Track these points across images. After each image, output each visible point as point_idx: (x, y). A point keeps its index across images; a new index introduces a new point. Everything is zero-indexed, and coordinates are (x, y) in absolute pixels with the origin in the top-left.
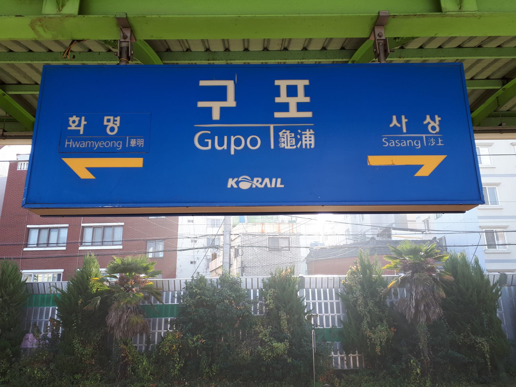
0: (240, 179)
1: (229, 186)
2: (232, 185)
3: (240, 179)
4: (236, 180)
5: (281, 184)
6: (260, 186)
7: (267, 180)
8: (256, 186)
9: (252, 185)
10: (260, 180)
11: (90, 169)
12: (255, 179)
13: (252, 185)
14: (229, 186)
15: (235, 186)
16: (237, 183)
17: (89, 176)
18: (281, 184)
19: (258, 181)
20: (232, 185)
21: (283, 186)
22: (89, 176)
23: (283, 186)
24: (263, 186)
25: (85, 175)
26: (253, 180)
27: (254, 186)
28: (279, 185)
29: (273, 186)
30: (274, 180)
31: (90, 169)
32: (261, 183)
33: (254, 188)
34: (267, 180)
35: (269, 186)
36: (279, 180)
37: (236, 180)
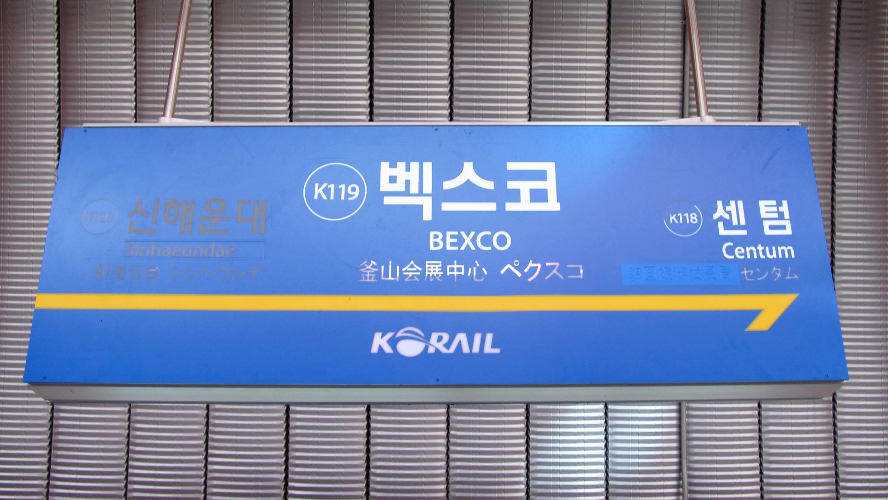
6: (444, 350)
7: (462, 337)
8: (437, 350)
9: (426, 348)
12: (435, 336)
13: (426, 348)
19: (440, 339)
24: (452, 349)
26: (427, 338)
27: (431, 350)
28: (488, 349)
32: (448, 346)
33: (431, 354)
34: (462, 337)
35: (466, 349)
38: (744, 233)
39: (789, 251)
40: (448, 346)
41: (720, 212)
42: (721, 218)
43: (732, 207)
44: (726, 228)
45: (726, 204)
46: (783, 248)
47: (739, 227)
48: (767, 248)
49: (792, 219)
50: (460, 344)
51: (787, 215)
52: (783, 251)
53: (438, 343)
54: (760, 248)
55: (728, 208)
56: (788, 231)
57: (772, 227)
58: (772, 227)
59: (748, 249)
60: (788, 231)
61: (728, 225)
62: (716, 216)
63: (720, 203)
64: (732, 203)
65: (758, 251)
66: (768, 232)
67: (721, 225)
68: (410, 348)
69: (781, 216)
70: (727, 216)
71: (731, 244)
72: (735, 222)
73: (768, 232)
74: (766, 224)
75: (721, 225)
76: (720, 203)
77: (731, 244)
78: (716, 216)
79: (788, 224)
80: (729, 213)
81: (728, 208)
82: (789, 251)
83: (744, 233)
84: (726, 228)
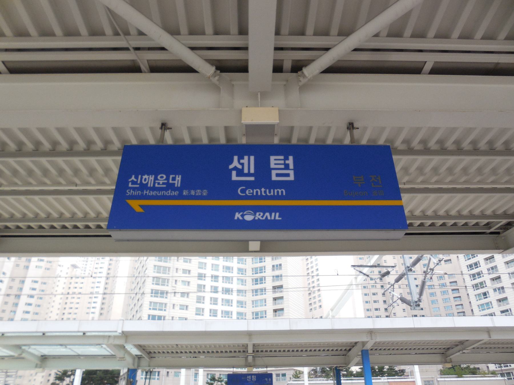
0: (245, 213)
1: (236, 218)
2: (238, 218)
6: (261, 219)
7: (267, 214)
9: (255, 218)
10: (262, 214)
12: (258, 214)
14: (236, 218)
15: (241, 218)
16: (242, 216)
18: (279, 217)
19: (260, 215)
20: (238, 218)
21: (280, 219)
23: (280, 219)
24: (264, 218)
26: (255, 214)
27: (256, 218)
28: (277, 218)
29: (273, 218)
30: (273, 214)
32: (262, 217)
35: (269, 218)
36: (277, 214)
37: (241, 213)
38: (252, 179)
39: (282, 192)
40: (262, 217)
41: (235, 163)
42: (235, 168)
43: (245, 161)
44: (237, 175)
45: (241, 158)
46: (279, 190)
47: (249, 175)
48: (268, 191)
49: (295, 169)
50: (267, 217)
51: (291, 166)
52: (278, 192)
53: (259, 216)
54: (263, 190)
55: (242, 161)
56: (292, 178)
57: (278, 175)
58: (278, 175)
59: (255, 191)
60: (292, 178)
61: (240, 173)
62: (231, 167)
63: (236, 158)
64: (246, 158)
65: (261, 192)
66: (274, 178)
67: (234, 173)
68: (249, 218)
69: (287, 167)
70: (240, 167)
71: (244, 187)
72: (246, 171)
73: (274, 178)
74: (274, 173)
75: (234, 173)
76: (236, 158)
77: (244, 187)
78: (231, 167)
79: (292, 173)
80: (242, 164)
81: (242, 161)
82: (282, 192)
83: (252, 179)
84: (237, 175)
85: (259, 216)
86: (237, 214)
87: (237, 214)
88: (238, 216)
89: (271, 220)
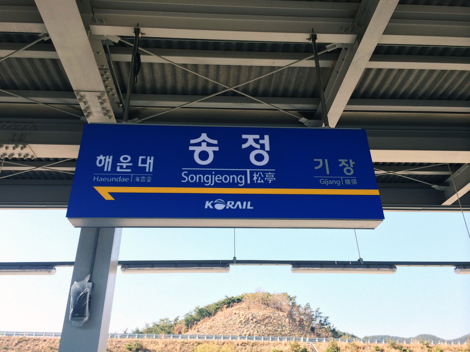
0: (215, 202)
1: (206, 207)
3: (215, 202)
4: (212, 202)
5: (250, 206)
6: (232, 208)
7: (239, 203)
9: (226, 207)
11: (111, 194)
12: (229, 202)
13: (226, 207)
14: (206, 207)
15: (211, 207)
16: (213, 205)
17: (111, 198)
18: (250, 206)
19: (231, 203)
21: (252, 208)
22: (111, 198)
23: (252, 208)
24: (235, 207)
25: (108, 198)
26: (226, 203)
27: (227, 207)
28: (249, 207)
29: (244, 207)
30: (245, 203)
31: (111, 194)
32: (234, 206)
35: (240, 207)
36: (249, 203)
37: (212, 202)
40: (234, 206)
53: (230, 205)
68: (220, 207)
85: (230, 205)
86: (207, 202)
87: (207, 202)
88: (208, 204)
89: (242, 209)
